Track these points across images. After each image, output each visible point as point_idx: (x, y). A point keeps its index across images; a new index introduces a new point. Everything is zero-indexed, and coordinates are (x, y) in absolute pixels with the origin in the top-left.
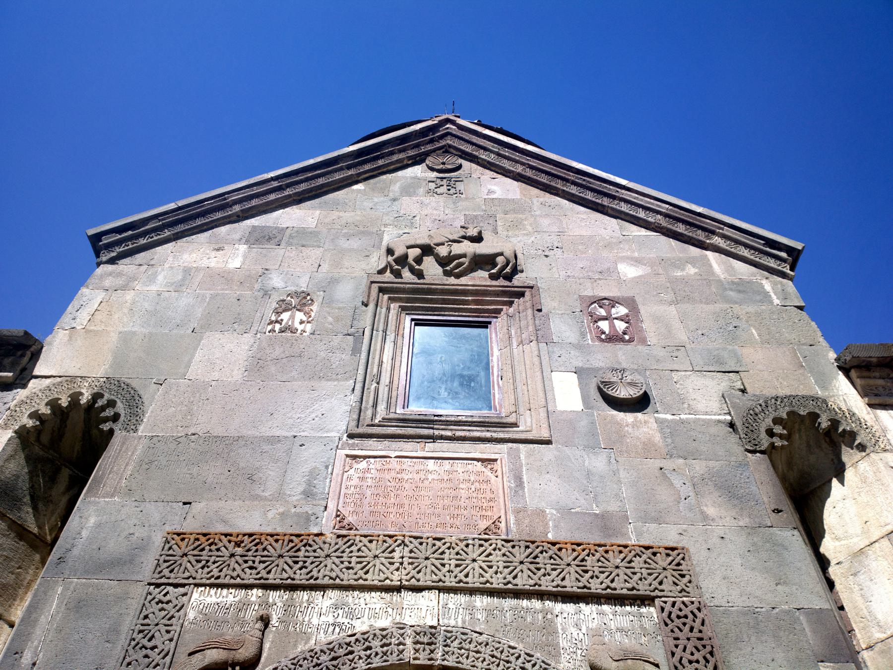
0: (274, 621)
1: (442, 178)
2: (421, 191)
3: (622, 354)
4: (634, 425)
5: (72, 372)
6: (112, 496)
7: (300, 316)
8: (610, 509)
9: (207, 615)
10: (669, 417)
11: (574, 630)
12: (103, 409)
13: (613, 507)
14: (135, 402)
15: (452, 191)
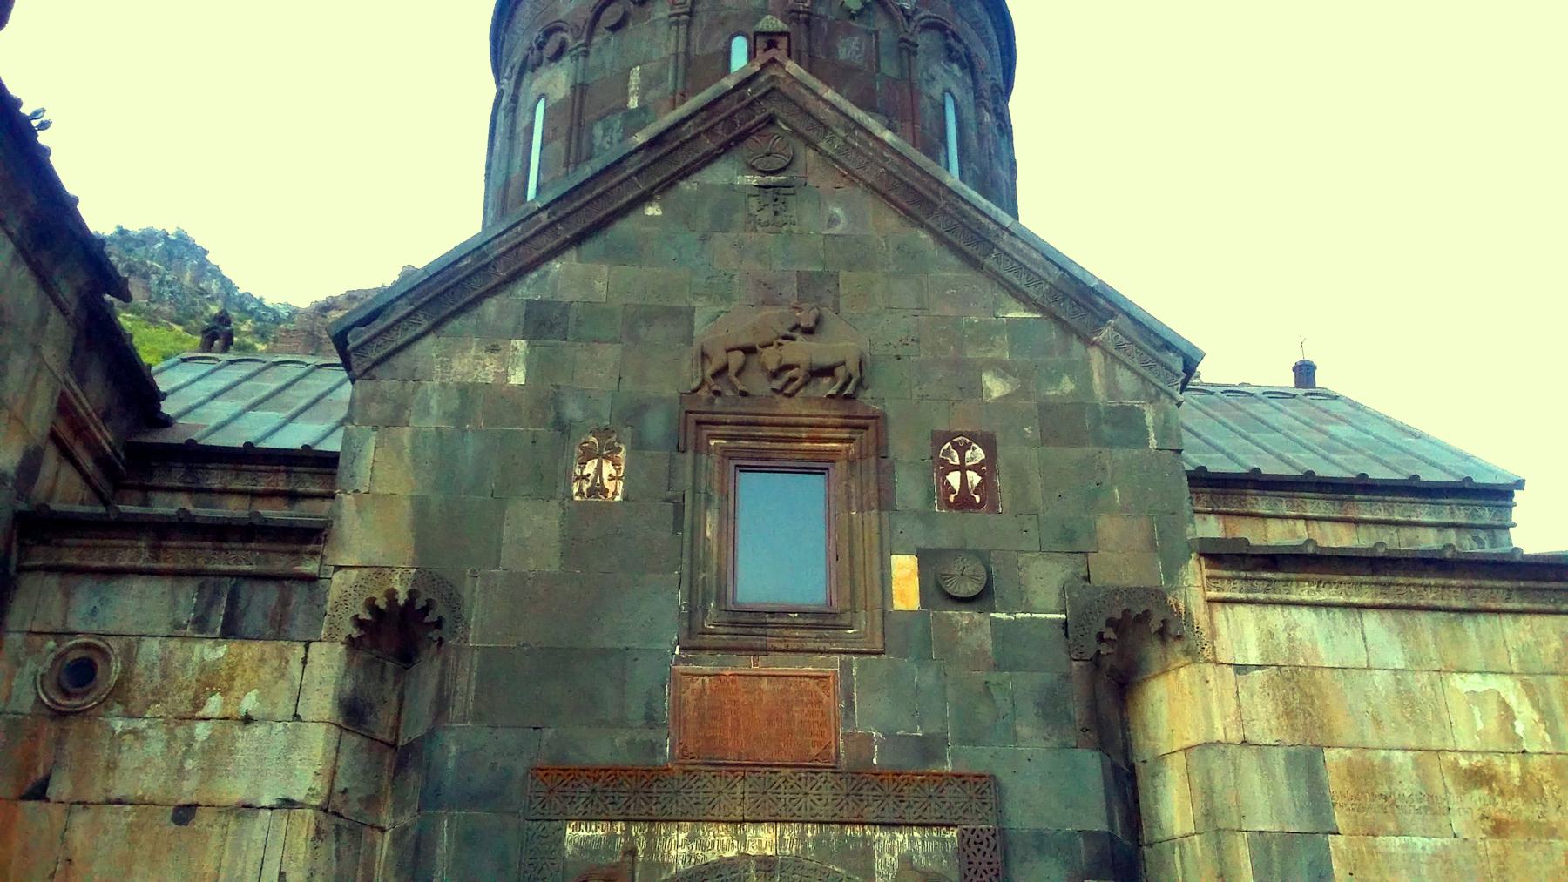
0: (640, 854)
1: (767, 187)
2: (739, 217)
3: (972, 527)
4: (968, 629)
5: (377, 561)
6: (464, 721)
7: (608, 468)
8: (932, 731)
9: (583, 847)
10: (1004, 616)
11: (888, 856)
12: (426, 610)
13: (934, 728)
14: (454, 602)
15: (779, 219)
